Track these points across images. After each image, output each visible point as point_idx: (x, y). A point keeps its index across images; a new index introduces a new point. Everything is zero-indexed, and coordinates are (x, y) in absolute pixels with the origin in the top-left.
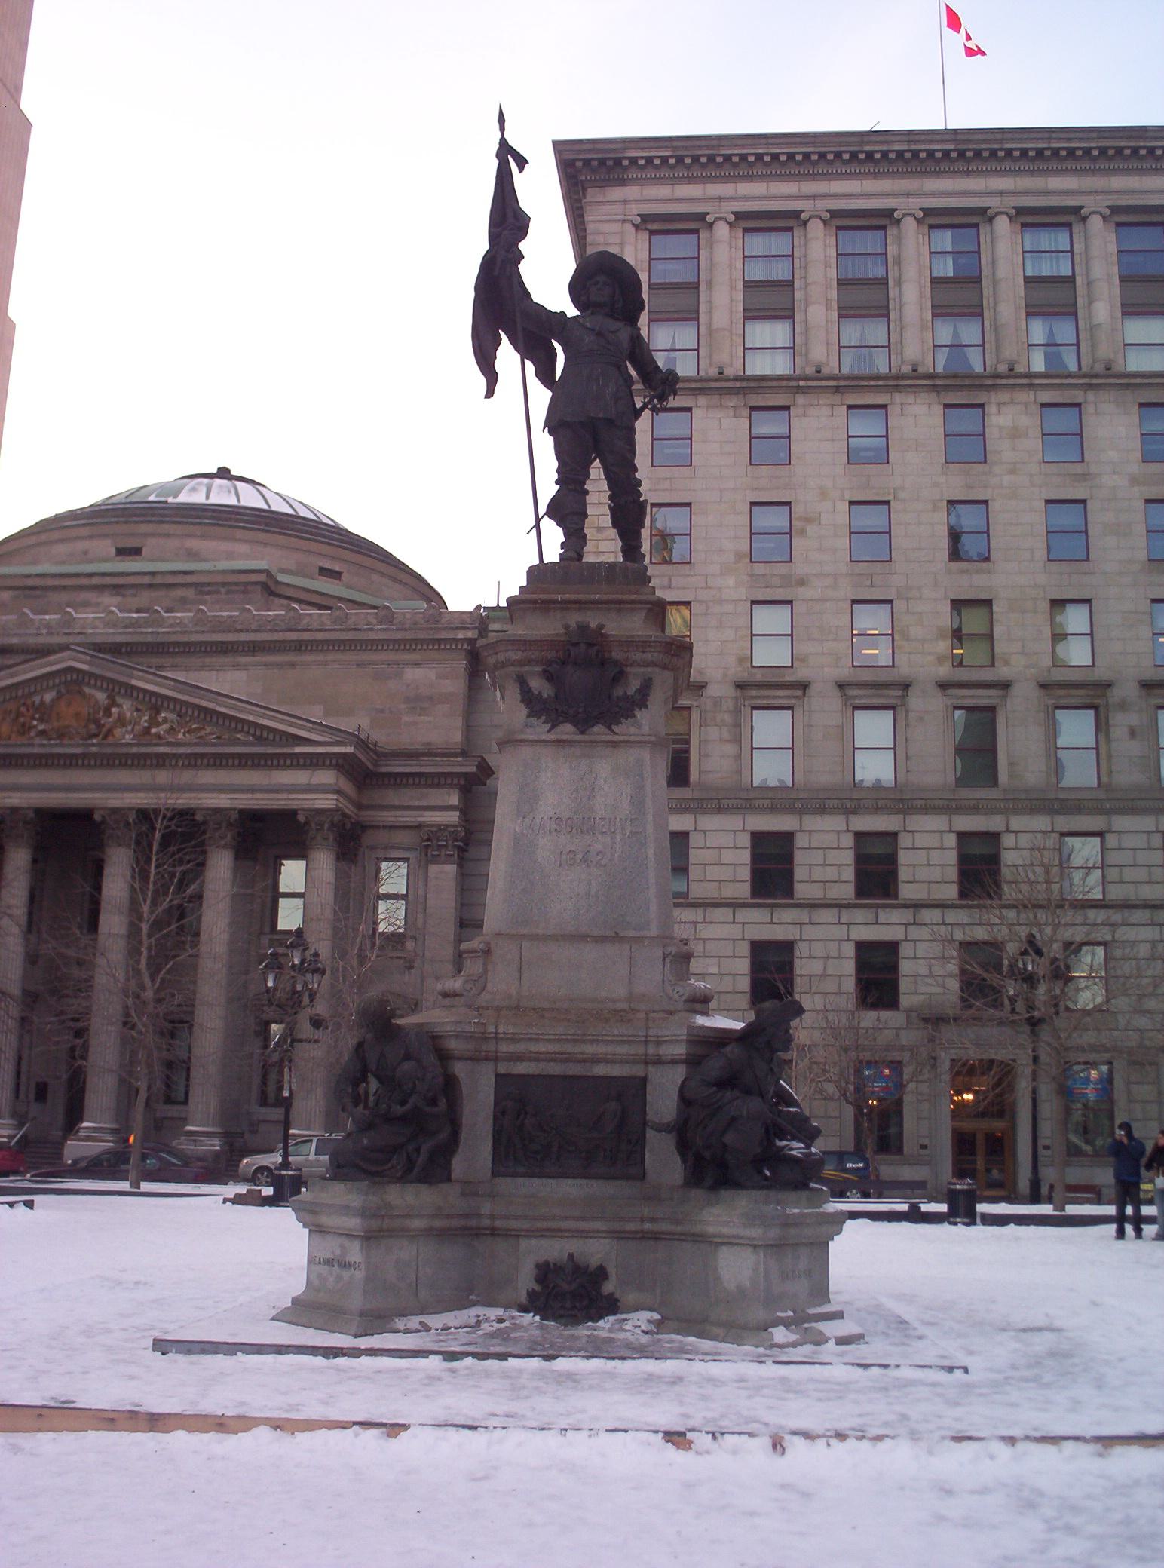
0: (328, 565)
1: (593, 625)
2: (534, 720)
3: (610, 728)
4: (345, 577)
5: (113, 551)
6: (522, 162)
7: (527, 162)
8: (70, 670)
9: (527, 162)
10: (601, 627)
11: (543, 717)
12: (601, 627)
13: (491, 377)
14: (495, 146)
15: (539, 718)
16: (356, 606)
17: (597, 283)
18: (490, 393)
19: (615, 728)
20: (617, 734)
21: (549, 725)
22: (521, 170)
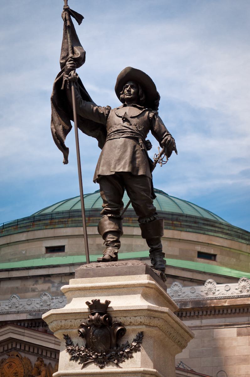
0: (205, 250)
1: (103, 301)
2: (73, 362)
3: (117, 365)
4: (218, 257)
5: (44, 250)
6: (80, 19)
7: (83, 18)
8: (11, 340)
9: (83, 18)
10: (108, 303)
11: (79, 361)
12: (108, 303)
13: (65, 150)
14: (60, 10)
15: (76, 361)
16: (227, 280)
17: (127, 87)
18: (66, 162)
19: (120, 365)
20: (122, 368)
21: (83, 364)
22: (79, 23)
